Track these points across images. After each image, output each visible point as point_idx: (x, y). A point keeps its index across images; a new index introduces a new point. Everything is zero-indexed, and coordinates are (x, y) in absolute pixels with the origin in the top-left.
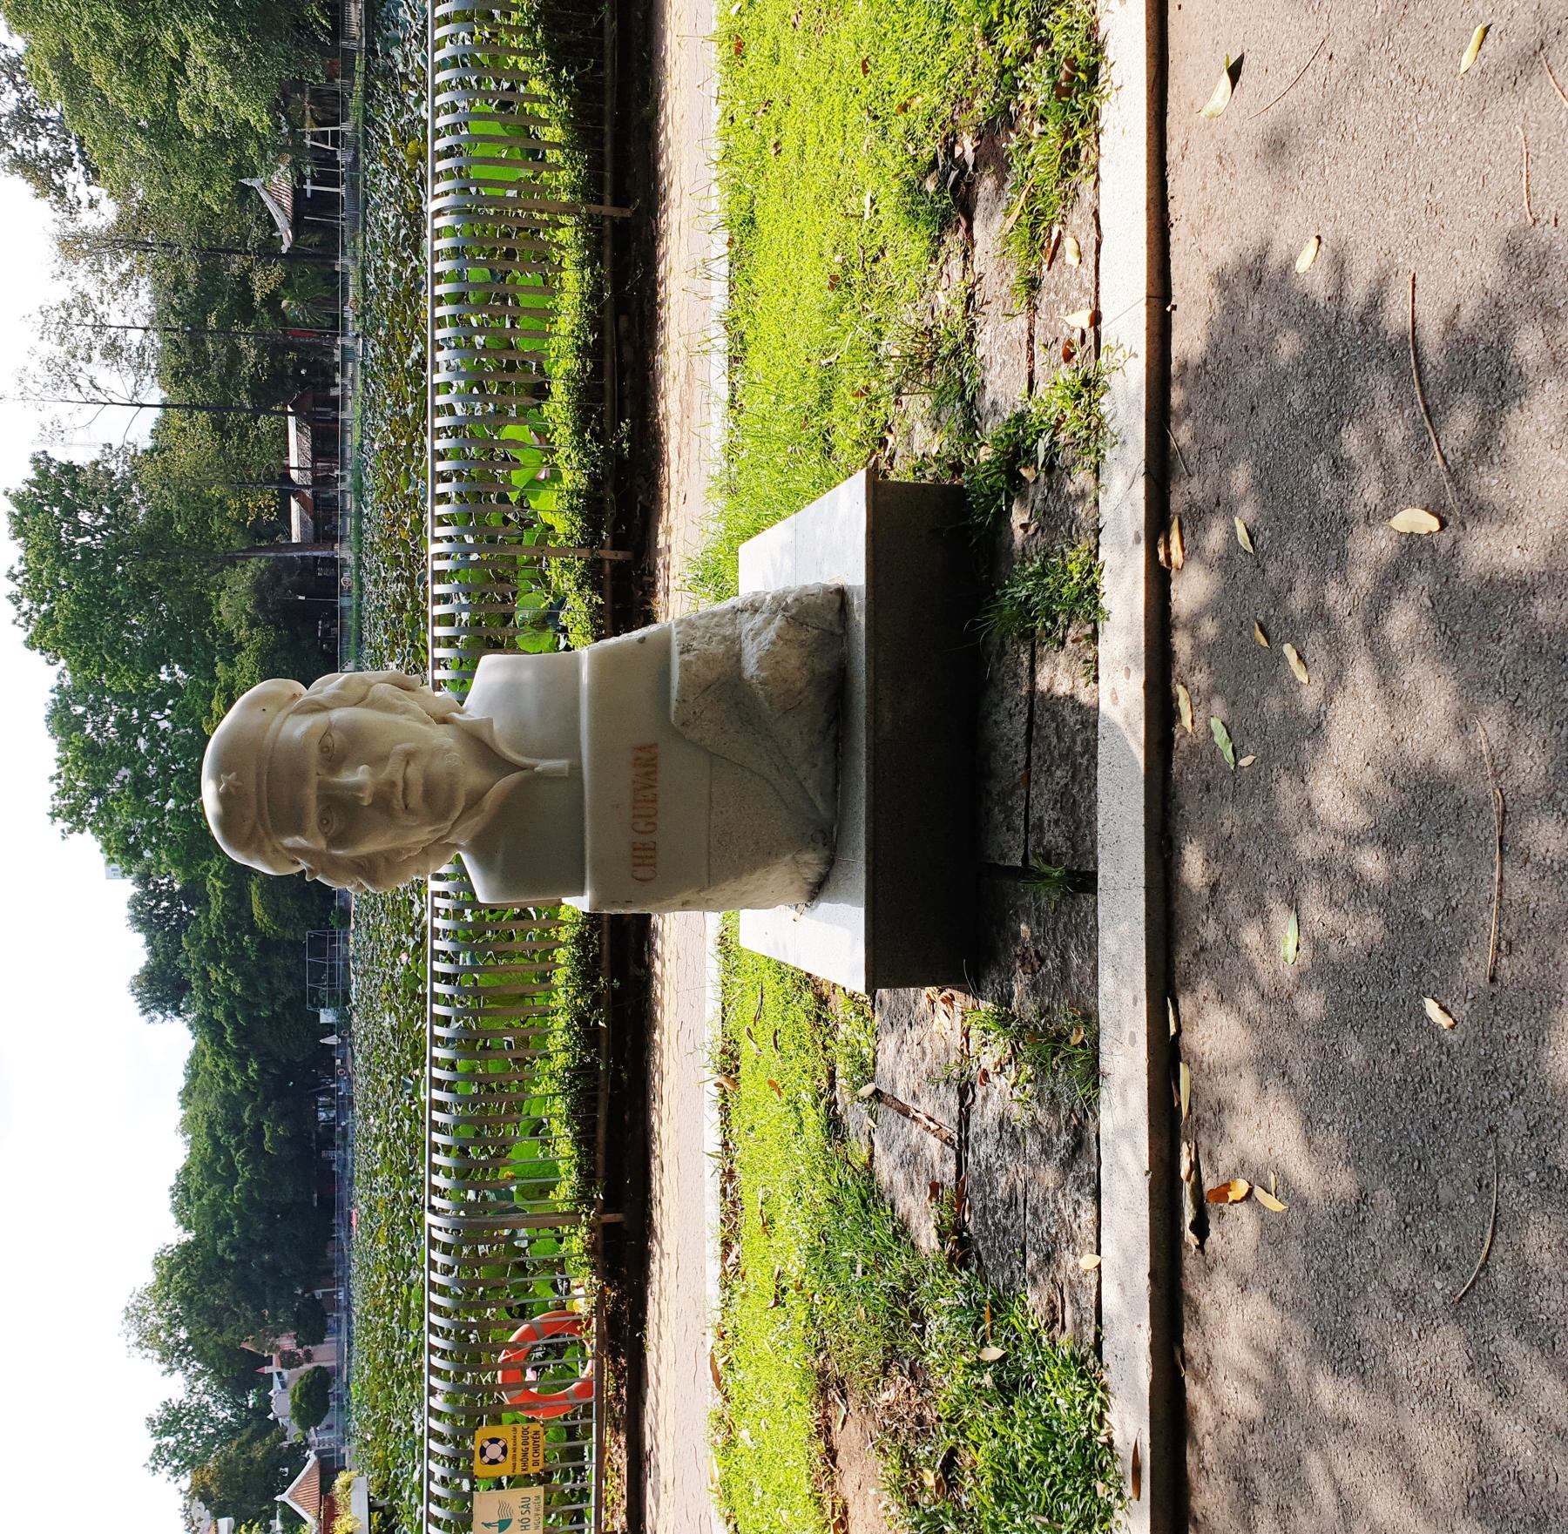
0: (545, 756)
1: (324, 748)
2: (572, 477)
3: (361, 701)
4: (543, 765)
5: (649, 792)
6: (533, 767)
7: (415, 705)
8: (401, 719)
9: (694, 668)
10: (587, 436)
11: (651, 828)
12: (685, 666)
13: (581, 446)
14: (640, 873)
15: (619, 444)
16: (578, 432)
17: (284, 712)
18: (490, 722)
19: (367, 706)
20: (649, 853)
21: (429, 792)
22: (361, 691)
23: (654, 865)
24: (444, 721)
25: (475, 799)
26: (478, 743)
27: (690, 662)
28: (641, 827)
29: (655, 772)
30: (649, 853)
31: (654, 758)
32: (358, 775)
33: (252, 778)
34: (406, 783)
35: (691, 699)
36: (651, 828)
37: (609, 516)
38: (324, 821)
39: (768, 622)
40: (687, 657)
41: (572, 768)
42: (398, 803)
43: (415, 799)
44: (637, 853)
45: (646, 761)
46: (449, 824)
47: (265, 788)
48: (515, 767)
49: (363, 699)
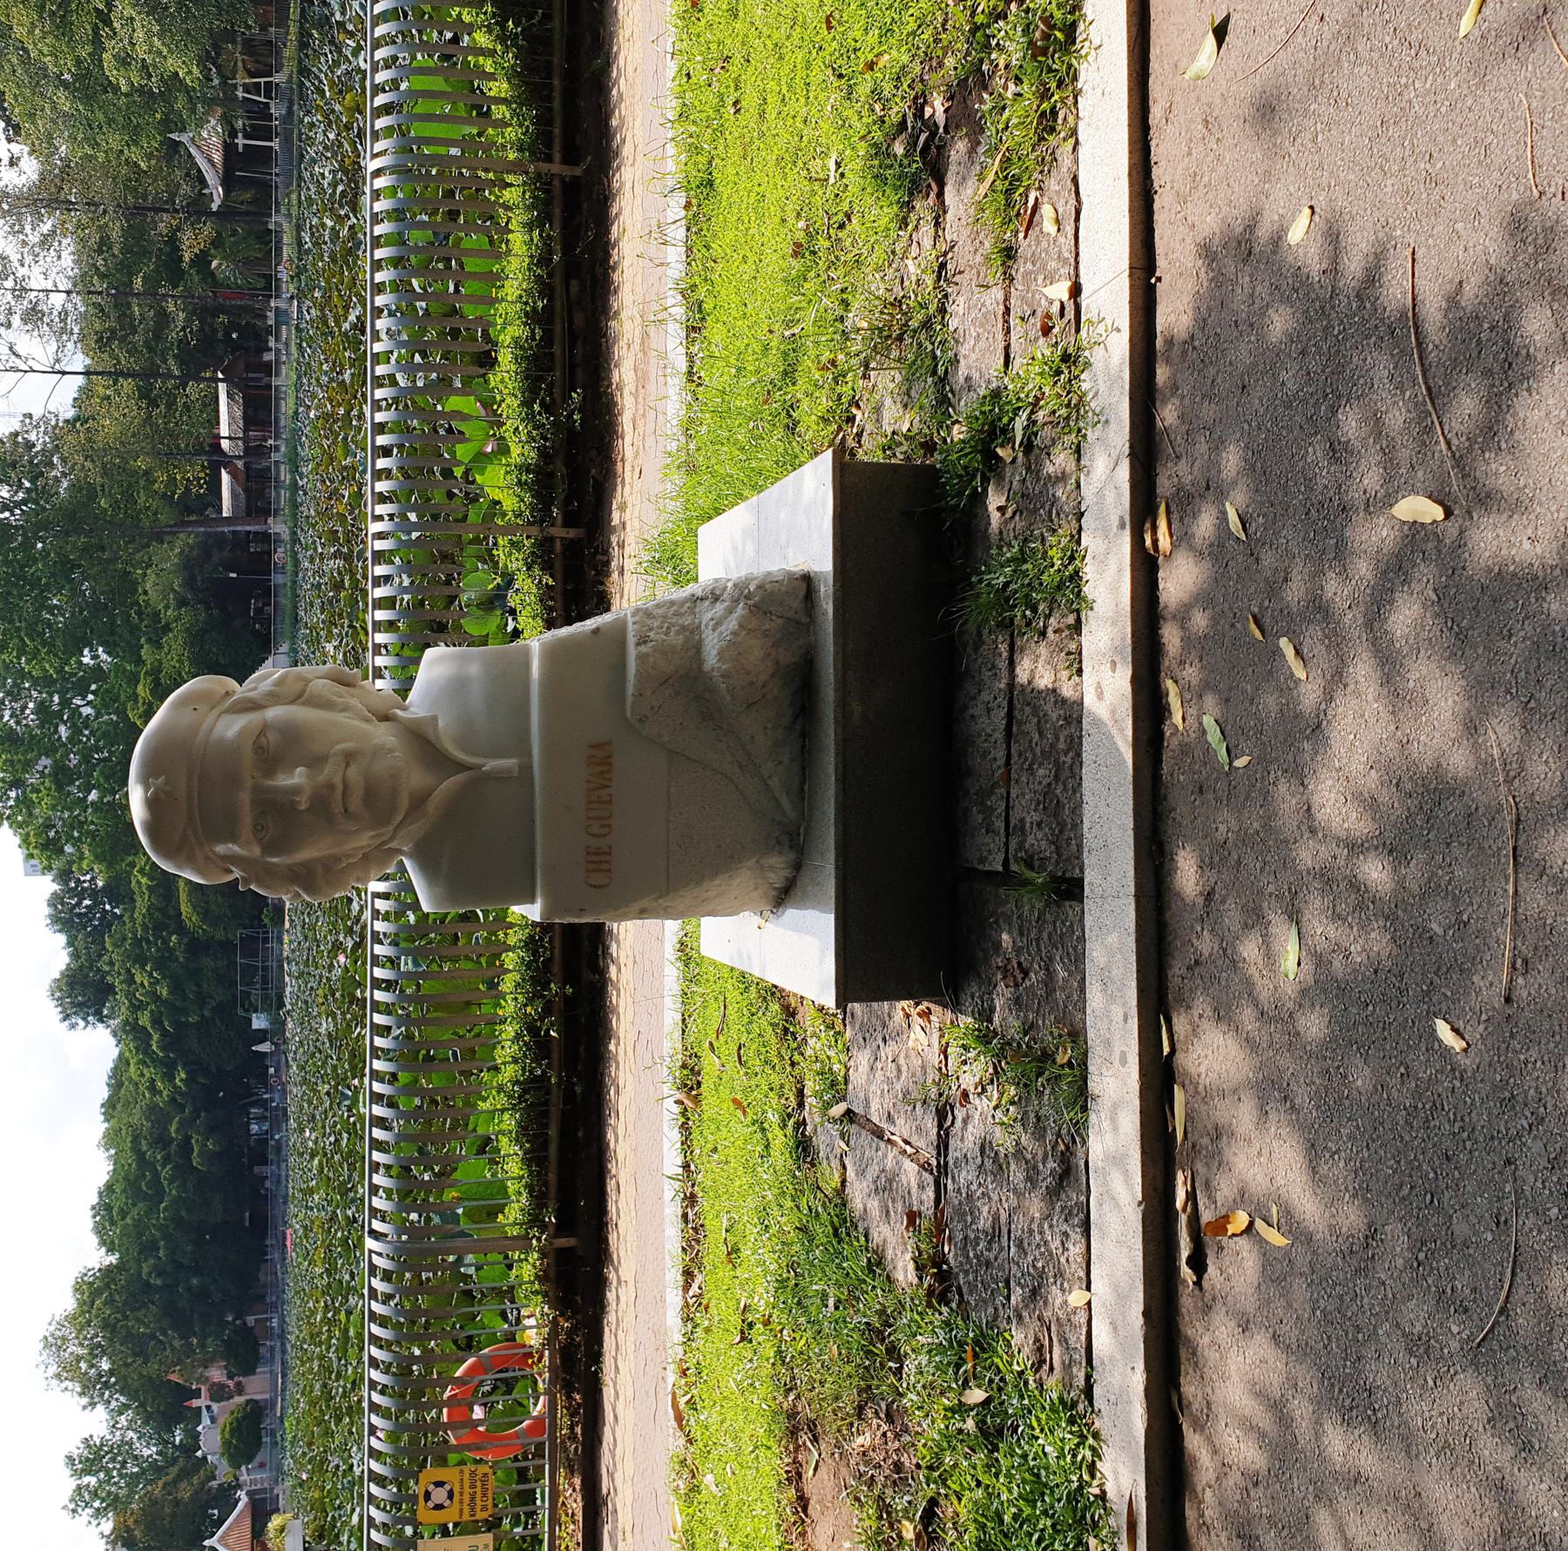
0: (494, 755)
1: (259, 749)
2: (520, 451)
3: (296, 699)
4: (491, 764)
6: (480, 767)
7: (354, 702)
8: (340, 717)
9: (652, 660)
10: (536, 407)
11: (603, 831)
12: (641, 658)
13: (530, 418)
15: (570, 416)
16: (527, 404)
17: (215, 713)
18: (434, 719)
19: (304, 704)
21: (370, 793)
22: (298, 686)
24: (386, 718)
25: (419, 801)
26: (420, 739)
28: (595, 829)
29: (609, 771)
30: (606, 858)
31: (609, 757)
32: (296, 778)
34: (345, 786)
36: (606, 830)
37: (560, 492)
38: (258, 828)
39: (730, 611)
40: (643, 649)
41: (521, 767)
42: (337, 808)
43: (355, 803)
45: (601, 760)
48: (463, 767)
49: (300, 696)
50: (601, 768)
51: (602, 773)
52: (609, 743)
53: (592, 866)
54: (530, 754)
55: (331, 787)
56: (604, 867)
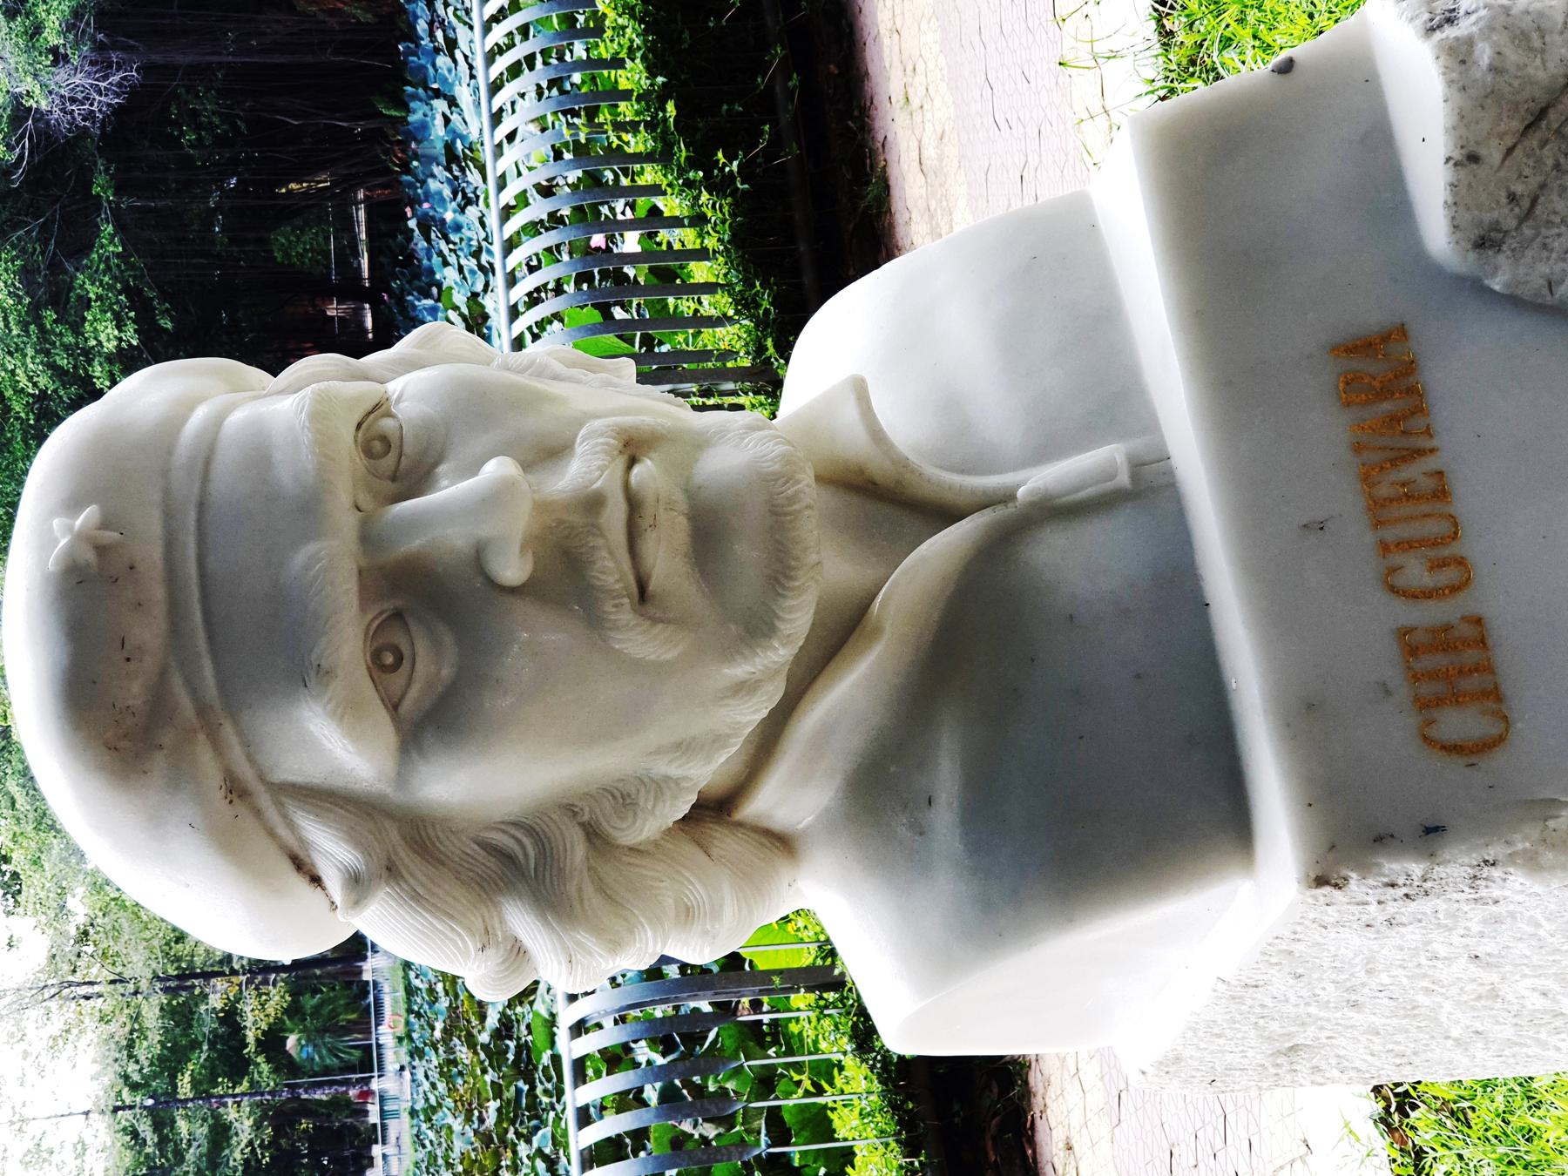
5: (1414, 471)
11: (1449, 575)
14: (1460, 723)
20: (1471, 656)
23: (1494, 694)
27: (1469, 42)
28: (1416, 572)
29: (1419, 410)
30: (1471, 656)
31: (1410, 367)
33: (153, 526)
35: (1492, 153)
36: (1449, 575)
38: (385, 661)
41: (1137, 466)
42: (611, 569)
43: (666, 558)
44: (1428, 662)
45: (1381, 381)
46: (779, 655)
47: (192, 569)
50: (1386, 406)
51: (1393, 420)
52: (1401, 332)
53: (1438, 687)
54: (1151, 425)
55: (593, 503)
56: (1471, 683)
